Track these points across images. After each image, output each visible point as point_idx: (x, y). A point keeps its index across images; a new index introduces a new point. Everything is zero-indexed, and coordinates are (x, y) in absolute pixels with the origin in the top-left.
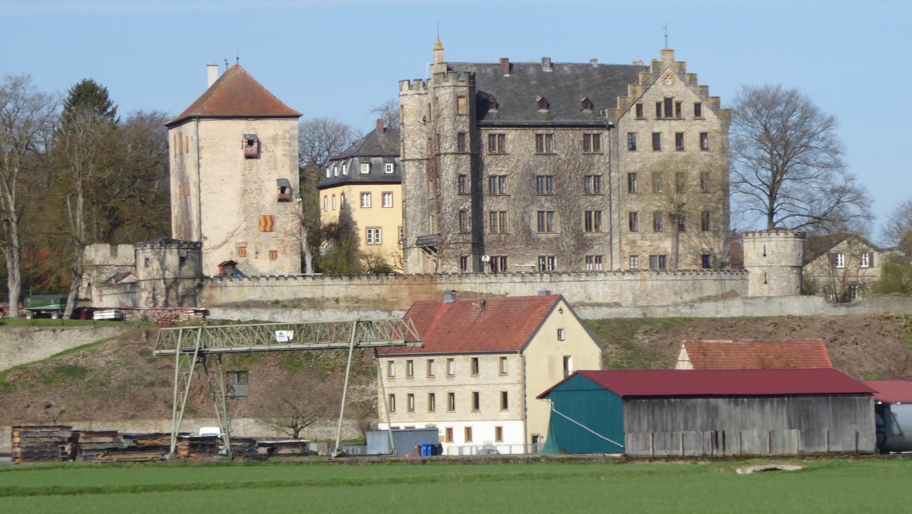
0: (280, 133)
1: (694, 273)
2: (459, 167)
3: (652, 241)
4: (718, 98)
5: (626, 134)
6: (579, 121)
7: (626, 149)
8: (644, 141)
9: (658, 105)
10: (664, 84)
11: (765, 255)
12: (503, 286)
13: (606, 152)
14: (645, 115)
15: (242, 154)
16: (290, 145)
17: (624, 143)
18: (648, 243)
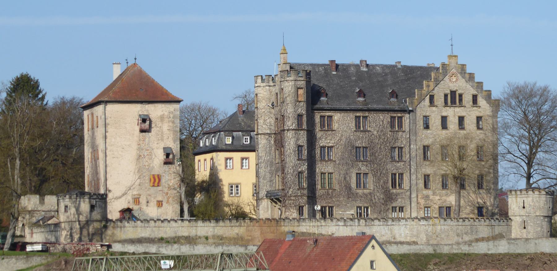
0: (166, 113)
1: (472, 220)
2: (298, 139)
4: (490, 91)
5: (422, 117)
6: (388, 107)
7: (422, 128)
8: (435, 122)
9: (446, 96)
10: (450, 80)
11: (524, 207)
13: (408, 130)
14: (436, 103)
15: (137, 128)
16: (173, 122)
17: (420, 123)
18: (438, 198)
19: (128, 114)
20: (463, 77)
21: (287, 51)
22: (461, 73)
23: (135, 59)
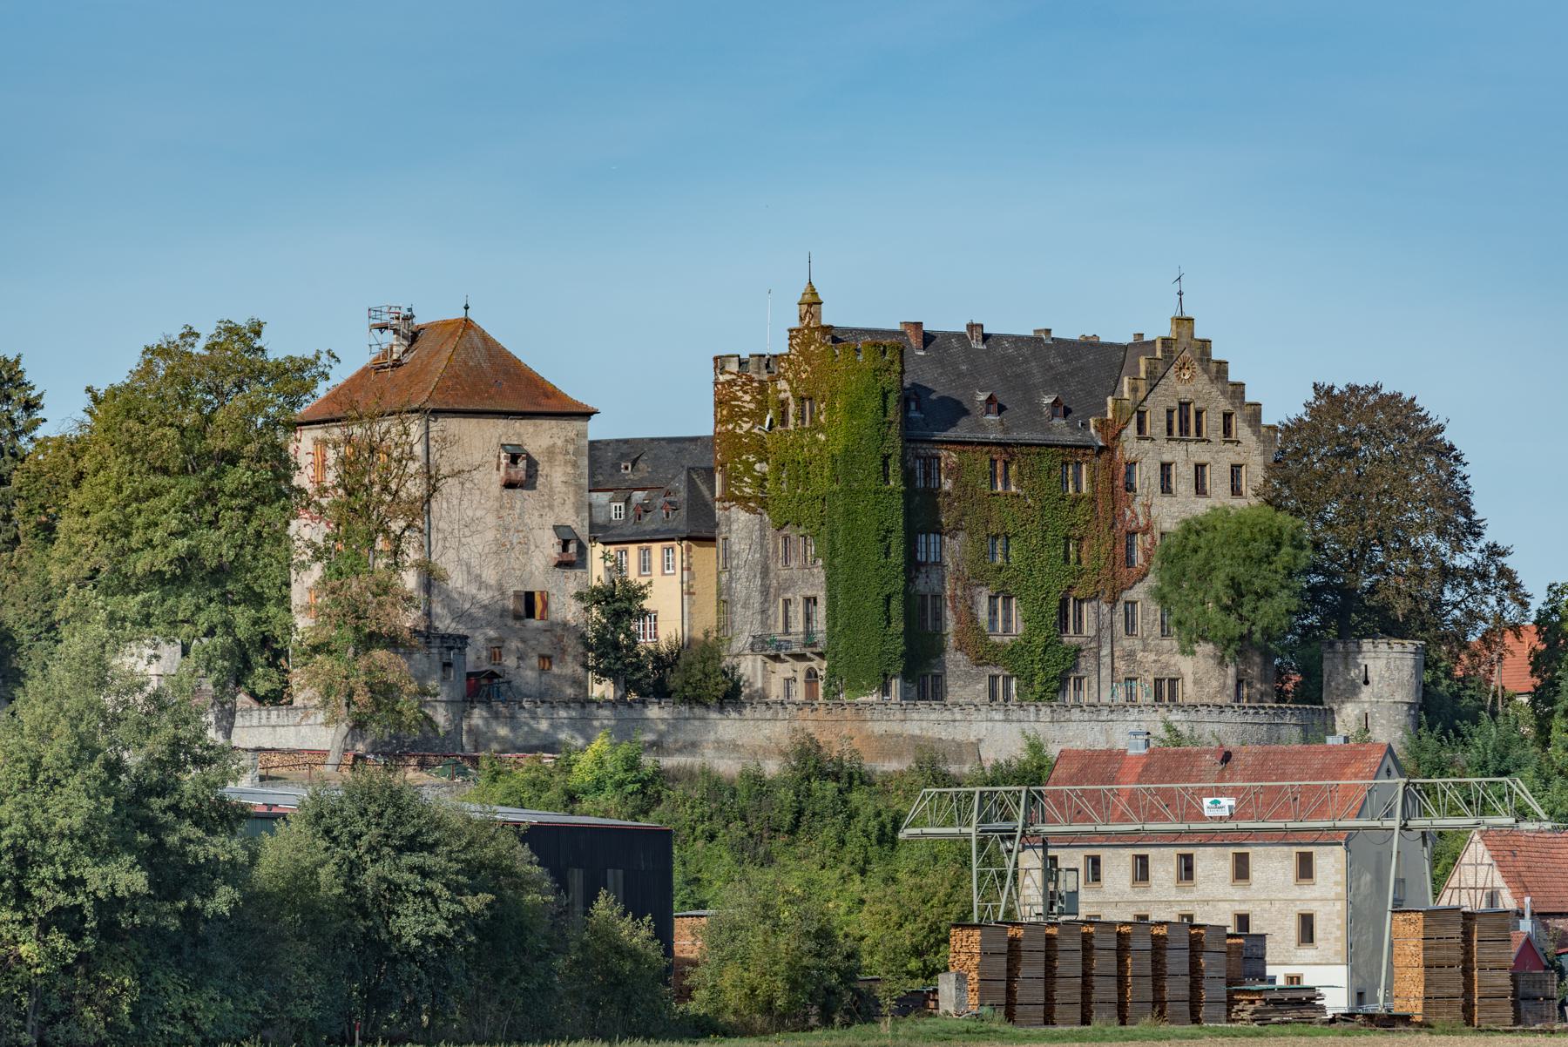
0: (560, 443)
3: (1158, 653)
9: (1170, 412)
12: (974, 726)
15: (498, 477)
16: (575, 465)
18: (1152, 657)
19: (477, 442)
20: (1206, 371)
21: (821, 297)
22: (1201, 360)
23: (467, 308)
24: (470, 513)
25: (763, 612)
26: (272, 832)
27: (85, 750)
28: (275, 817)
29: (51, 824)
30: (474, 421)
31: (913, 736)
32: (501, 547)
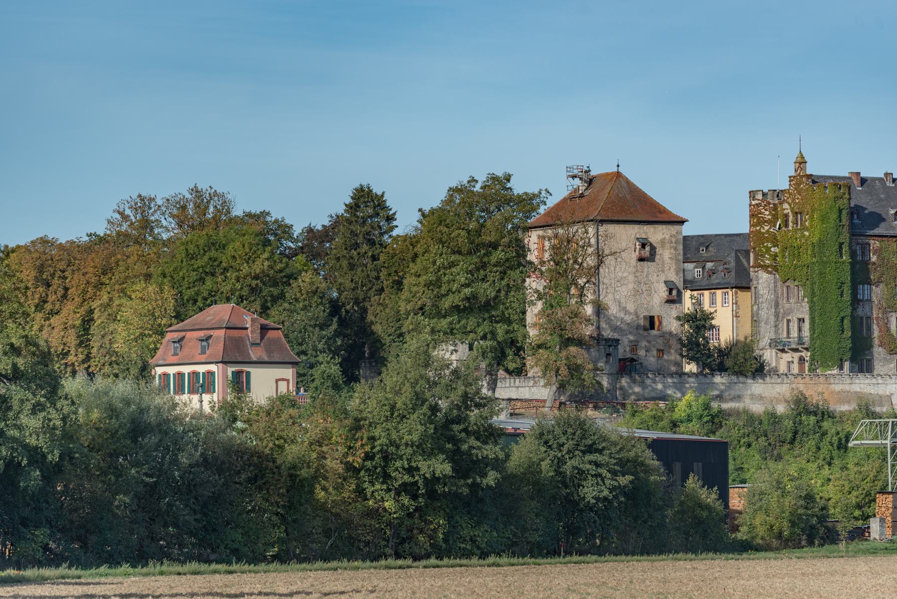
0: (667, 237)
12: (889, 387)
15: (635, 255)
16: (676, 249)
19: (624, 237)
21: (806, 159)
24: (620, 274)
25: (776, 326)
26: (517, 443)
27: (419, 400)
28: (518, 435)
29: (401, 438)
30: (622, 226)
31: (856, 392)
32: (637, 293)
